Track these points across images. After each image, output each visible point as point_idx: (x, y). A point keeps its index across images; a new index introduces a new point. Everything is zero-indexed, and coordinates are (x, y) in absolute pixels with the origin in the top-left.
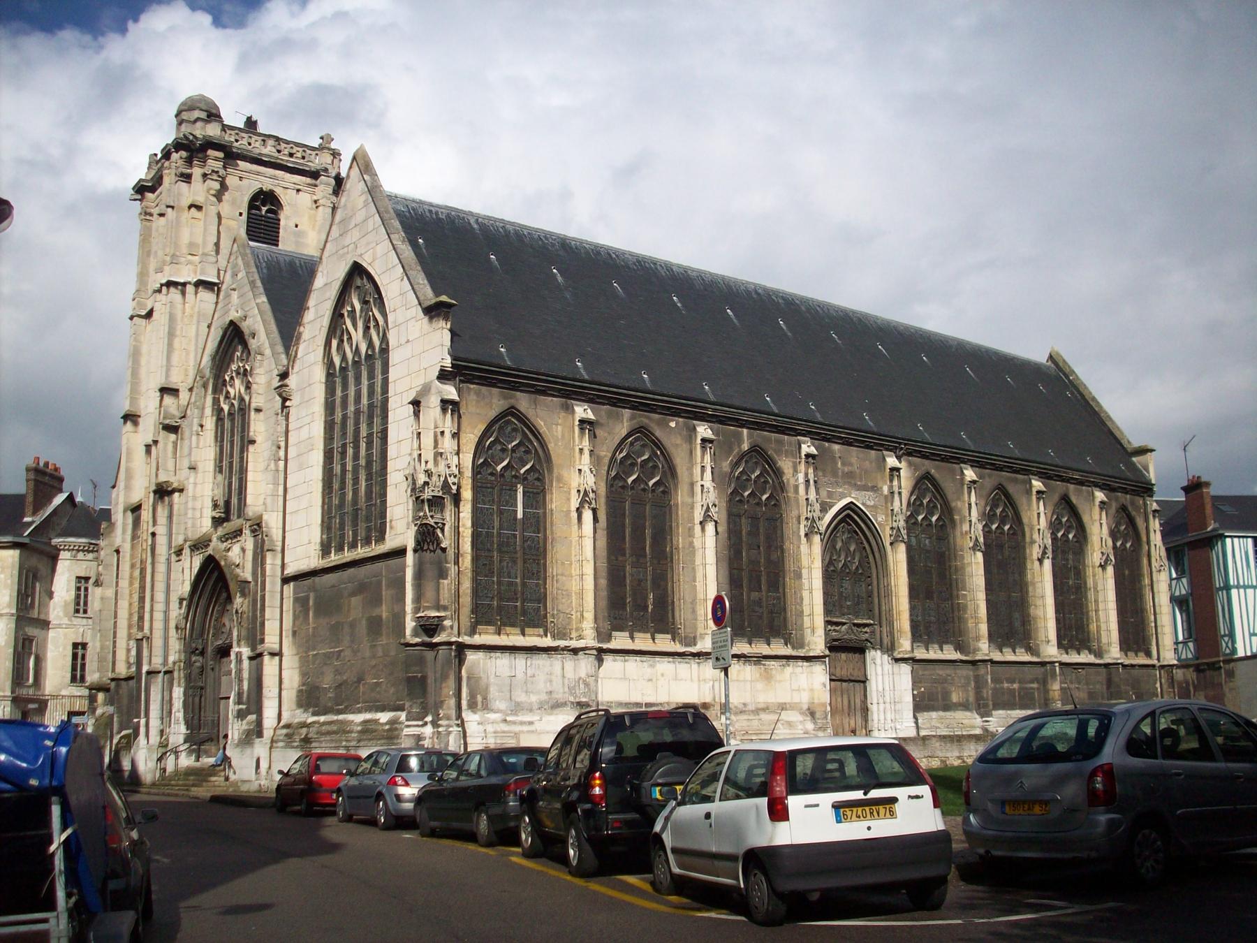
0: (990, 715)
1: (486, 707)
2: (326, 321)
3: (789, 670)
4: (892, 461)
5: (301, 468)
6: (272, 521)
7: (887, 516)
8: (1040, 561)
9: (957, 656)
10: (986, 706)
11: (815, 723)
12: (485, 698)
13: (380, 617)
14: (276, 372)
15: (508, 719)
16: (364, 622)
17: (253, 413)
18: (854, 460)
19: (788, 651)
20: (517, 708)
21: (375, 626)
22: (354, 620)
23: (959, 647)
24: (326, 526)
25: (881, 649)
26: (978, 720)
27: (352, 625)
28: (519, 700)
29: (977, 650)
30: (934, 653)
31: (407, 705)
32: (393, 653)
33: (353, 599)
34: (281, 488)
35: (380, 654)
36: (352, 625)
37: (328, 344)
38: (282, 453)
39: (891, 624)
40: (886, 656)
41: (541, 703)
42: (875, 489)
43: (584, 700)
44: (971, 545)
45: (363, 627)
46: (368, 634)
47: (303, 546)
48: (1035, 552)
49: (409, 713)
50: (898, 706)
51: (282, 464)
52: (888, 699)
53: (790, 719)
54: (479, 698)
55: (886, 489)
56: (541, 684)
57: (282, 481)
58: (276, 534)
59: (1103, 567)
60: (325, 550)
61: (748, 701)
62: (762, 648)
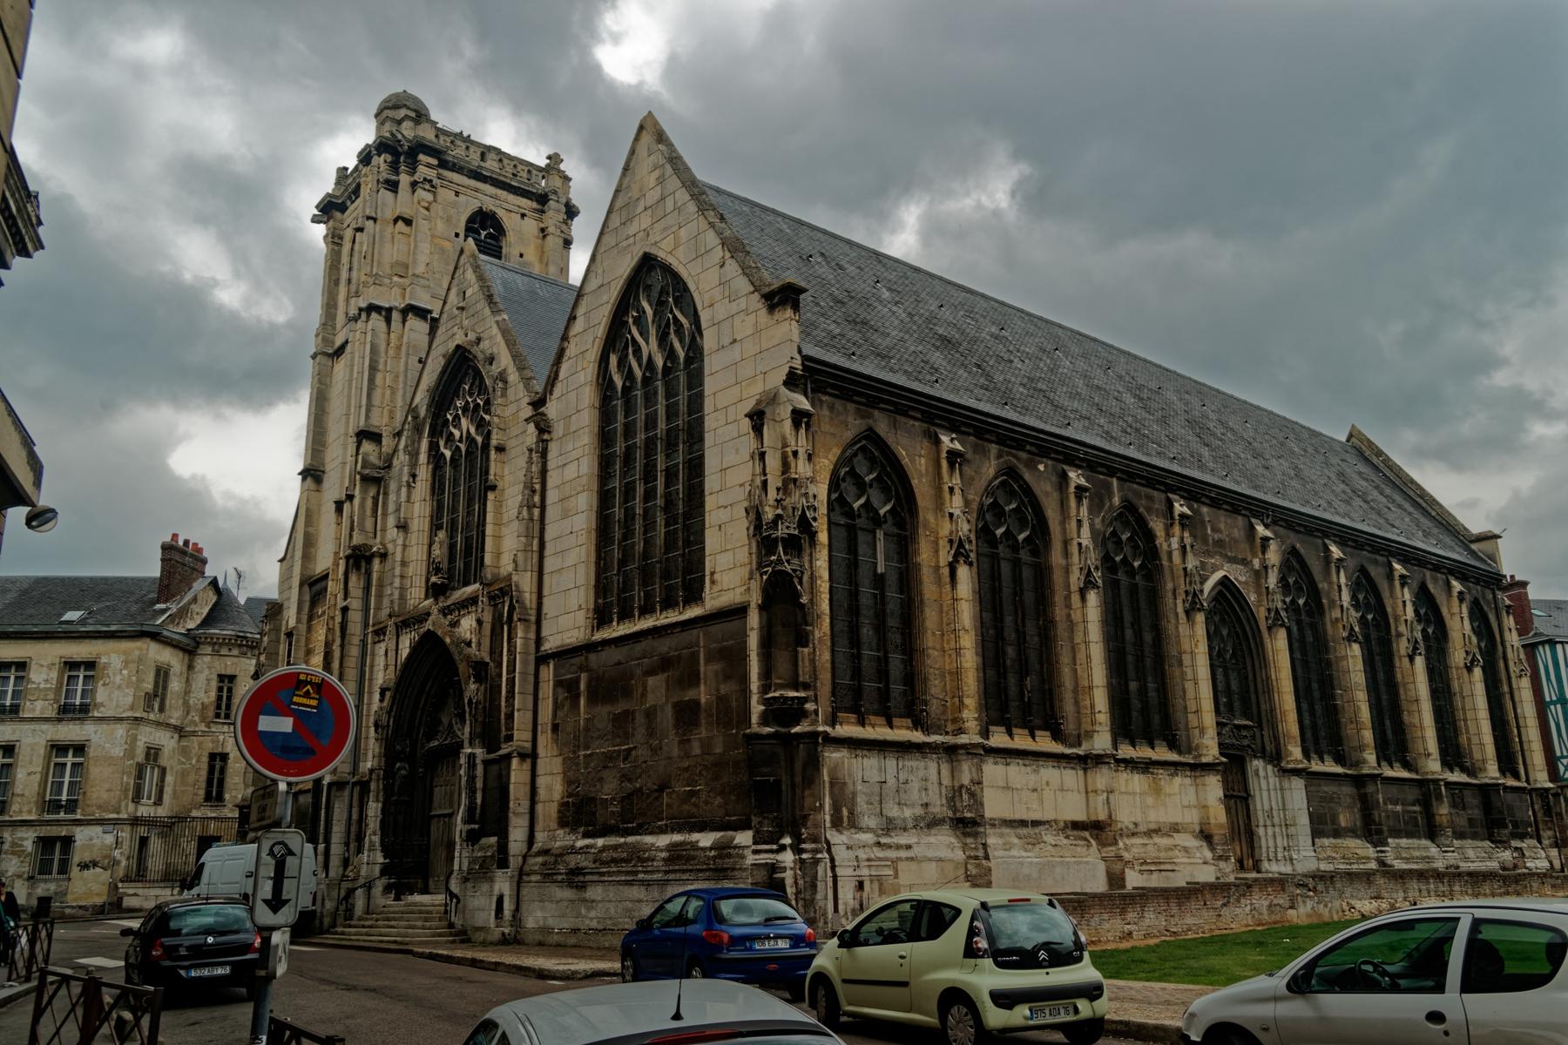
0: (1387, 844)
1: (854, 825)
2: (601, 331)
3: (1178, 780)
4: (1261, 530)
5: (565, 515)
6: (526, 582)
7: (1259, 594)
8: (1411, 659)
9: (1339, 770)
10: (1379, 832)
11: (1212, 849)
12: (851, 813)
13: (697, 703)
14: (527, 400)
15: (883, 840)
16: (669, 709)
17: (493, 453)
18: (1222, 526)
19: (1173, 757)
20: (889, 826)
21: (687, 715)
22: (654, 707)
23: (1340, 759)
25: (1263, 757)
26: (1371, 851)
27: (650, 714)
28: (890, 815)
29: (1358, 763)
30: (1316, 766)
31: (755, 820)
32: (719, 750)
33: (651, 681)
34: (536, 542)
35: (697, 751)
36: (650, 714)
37: (604, 360)
38: (537, 499)
39: (1274, 727)
40: (1270, 768)
41: (916, 819)
42: (1244, 562)
43: (968, 815)
44: (1345, 634)
45: (667, 716)
46: (677, 725)
48: (1403, 647)
49: (757, 832)
50: (1292, 830)
51: (536, 512)
52: (1276, 820)
53: (1187, 844)
54: (845, 812)
55: (1256, 563)
56: (914, 794)
57: (537, 533)
58: (529, 598)
59: (1469, 669)
60: (601, 617)
61: (1139, 820)
62: (1144, 752)
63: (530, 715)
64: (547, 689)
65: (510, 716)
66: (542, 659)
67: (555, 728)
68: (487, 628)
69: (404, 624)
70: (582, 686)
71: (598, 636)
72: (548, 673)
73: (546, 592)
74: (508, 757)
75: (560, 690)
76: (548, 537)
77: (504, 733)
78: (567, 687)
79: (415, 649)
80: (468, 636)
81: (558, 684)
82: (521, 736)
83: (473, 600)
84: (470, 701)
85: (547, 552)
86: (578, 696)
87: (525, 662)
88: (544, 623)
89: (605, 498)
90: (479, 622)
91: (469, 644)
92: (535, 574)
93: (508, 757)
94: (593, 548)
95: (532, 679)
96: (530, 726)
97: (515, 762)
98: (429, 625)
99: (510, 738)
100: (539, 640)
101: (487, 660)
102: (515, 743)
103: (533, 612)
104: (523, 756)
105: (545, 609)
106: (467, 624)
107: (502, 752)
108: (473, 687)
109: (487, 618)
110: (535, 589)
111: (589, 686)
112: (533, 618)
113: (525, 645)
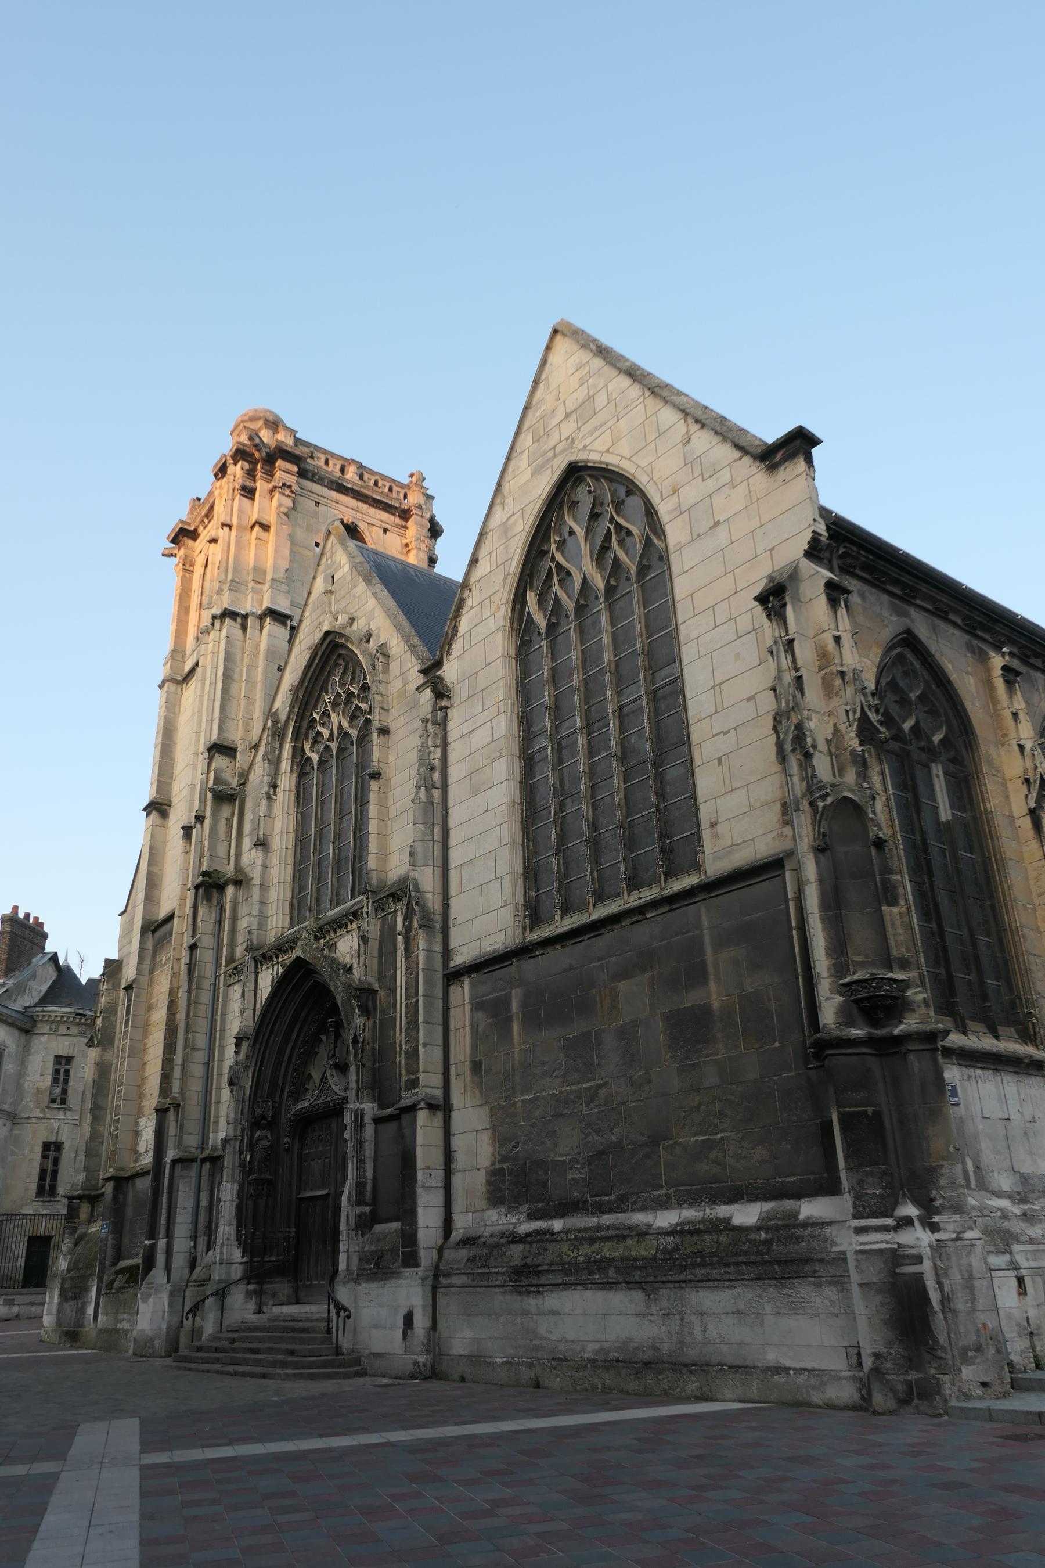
5: (475, 792)
6: (427, 880)
24: (531, 872)
34: (437, 830)
47: (485, 912)
57: (438, 819)
58: (434, 903)
60: (533, 913)
63: (438, 1052)
64: (462, 1016)
65: (413, 1055)
66: (453, 976)
67: (476, 1067)
68: (374, 944)
69: (262, 957)
70: (515, 1006)
71: (534, 936)
72: (462, 994)
73: (453, 890)
74: (412, 1109)
75: (480, 1015)
76: (452, 822)
77: (404, 1078)
78: (495, 1010)
79: (279, 986)
80: (348, 960)
81: (478, 1006)
82: (430, 1082)
83: (356, 915)
84: (355, 1041)
85: (452, 842)
86: (509, 1020)
87: (428, 981)
88: (453, 932)
89: (528, 763)
90: (364, 939)
91: (350, 970)
92: (438, 871)
93: (412, 1109)
94: (518, 826)
95: (439, 1004)
96: (439, 1068)
97: (422, 1116)
98: (297, 953)
99: (414, 1084)
100: (447, 954)
101: (376, 987)
102: (420, 1090)
103: (438, 918)
104: (432, 1107)
105: (453, 913)
106: (346, 946)
107: (404, 1103)
108: (359, 1021)
109: (373, 927)
110: (439, 889)
111: (524, 1005)
112: (438, 926)
113: (428, 959)
